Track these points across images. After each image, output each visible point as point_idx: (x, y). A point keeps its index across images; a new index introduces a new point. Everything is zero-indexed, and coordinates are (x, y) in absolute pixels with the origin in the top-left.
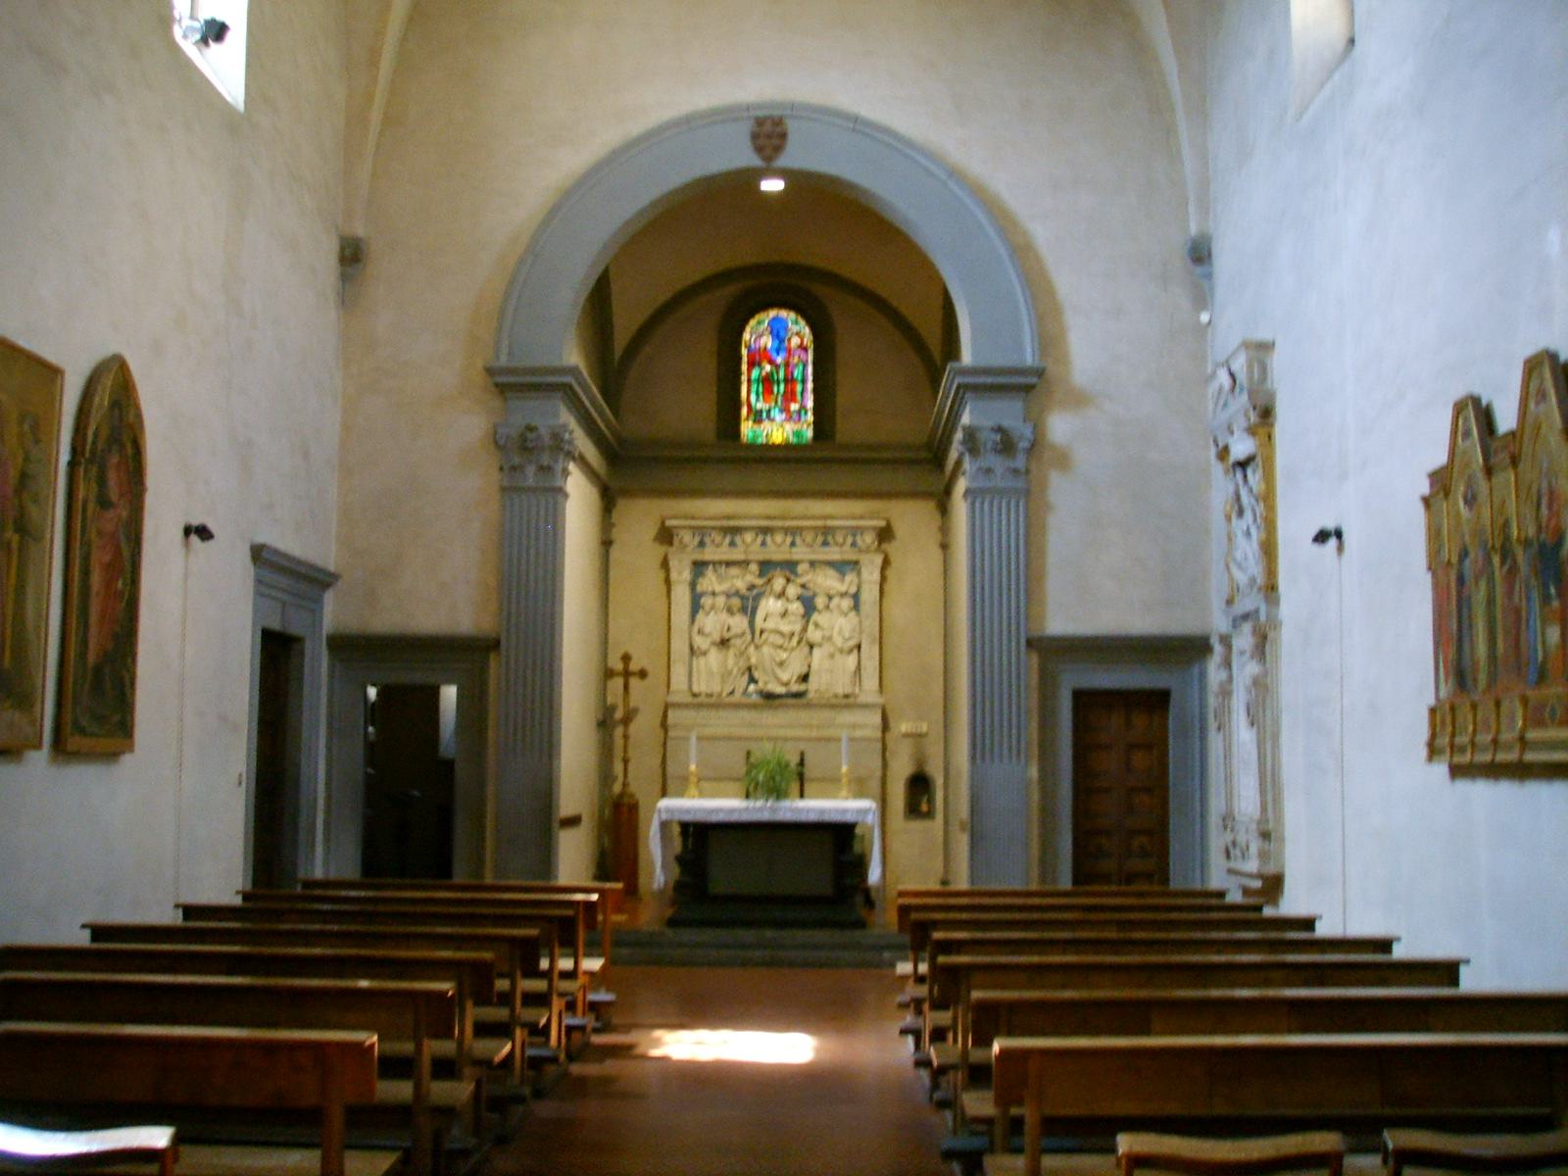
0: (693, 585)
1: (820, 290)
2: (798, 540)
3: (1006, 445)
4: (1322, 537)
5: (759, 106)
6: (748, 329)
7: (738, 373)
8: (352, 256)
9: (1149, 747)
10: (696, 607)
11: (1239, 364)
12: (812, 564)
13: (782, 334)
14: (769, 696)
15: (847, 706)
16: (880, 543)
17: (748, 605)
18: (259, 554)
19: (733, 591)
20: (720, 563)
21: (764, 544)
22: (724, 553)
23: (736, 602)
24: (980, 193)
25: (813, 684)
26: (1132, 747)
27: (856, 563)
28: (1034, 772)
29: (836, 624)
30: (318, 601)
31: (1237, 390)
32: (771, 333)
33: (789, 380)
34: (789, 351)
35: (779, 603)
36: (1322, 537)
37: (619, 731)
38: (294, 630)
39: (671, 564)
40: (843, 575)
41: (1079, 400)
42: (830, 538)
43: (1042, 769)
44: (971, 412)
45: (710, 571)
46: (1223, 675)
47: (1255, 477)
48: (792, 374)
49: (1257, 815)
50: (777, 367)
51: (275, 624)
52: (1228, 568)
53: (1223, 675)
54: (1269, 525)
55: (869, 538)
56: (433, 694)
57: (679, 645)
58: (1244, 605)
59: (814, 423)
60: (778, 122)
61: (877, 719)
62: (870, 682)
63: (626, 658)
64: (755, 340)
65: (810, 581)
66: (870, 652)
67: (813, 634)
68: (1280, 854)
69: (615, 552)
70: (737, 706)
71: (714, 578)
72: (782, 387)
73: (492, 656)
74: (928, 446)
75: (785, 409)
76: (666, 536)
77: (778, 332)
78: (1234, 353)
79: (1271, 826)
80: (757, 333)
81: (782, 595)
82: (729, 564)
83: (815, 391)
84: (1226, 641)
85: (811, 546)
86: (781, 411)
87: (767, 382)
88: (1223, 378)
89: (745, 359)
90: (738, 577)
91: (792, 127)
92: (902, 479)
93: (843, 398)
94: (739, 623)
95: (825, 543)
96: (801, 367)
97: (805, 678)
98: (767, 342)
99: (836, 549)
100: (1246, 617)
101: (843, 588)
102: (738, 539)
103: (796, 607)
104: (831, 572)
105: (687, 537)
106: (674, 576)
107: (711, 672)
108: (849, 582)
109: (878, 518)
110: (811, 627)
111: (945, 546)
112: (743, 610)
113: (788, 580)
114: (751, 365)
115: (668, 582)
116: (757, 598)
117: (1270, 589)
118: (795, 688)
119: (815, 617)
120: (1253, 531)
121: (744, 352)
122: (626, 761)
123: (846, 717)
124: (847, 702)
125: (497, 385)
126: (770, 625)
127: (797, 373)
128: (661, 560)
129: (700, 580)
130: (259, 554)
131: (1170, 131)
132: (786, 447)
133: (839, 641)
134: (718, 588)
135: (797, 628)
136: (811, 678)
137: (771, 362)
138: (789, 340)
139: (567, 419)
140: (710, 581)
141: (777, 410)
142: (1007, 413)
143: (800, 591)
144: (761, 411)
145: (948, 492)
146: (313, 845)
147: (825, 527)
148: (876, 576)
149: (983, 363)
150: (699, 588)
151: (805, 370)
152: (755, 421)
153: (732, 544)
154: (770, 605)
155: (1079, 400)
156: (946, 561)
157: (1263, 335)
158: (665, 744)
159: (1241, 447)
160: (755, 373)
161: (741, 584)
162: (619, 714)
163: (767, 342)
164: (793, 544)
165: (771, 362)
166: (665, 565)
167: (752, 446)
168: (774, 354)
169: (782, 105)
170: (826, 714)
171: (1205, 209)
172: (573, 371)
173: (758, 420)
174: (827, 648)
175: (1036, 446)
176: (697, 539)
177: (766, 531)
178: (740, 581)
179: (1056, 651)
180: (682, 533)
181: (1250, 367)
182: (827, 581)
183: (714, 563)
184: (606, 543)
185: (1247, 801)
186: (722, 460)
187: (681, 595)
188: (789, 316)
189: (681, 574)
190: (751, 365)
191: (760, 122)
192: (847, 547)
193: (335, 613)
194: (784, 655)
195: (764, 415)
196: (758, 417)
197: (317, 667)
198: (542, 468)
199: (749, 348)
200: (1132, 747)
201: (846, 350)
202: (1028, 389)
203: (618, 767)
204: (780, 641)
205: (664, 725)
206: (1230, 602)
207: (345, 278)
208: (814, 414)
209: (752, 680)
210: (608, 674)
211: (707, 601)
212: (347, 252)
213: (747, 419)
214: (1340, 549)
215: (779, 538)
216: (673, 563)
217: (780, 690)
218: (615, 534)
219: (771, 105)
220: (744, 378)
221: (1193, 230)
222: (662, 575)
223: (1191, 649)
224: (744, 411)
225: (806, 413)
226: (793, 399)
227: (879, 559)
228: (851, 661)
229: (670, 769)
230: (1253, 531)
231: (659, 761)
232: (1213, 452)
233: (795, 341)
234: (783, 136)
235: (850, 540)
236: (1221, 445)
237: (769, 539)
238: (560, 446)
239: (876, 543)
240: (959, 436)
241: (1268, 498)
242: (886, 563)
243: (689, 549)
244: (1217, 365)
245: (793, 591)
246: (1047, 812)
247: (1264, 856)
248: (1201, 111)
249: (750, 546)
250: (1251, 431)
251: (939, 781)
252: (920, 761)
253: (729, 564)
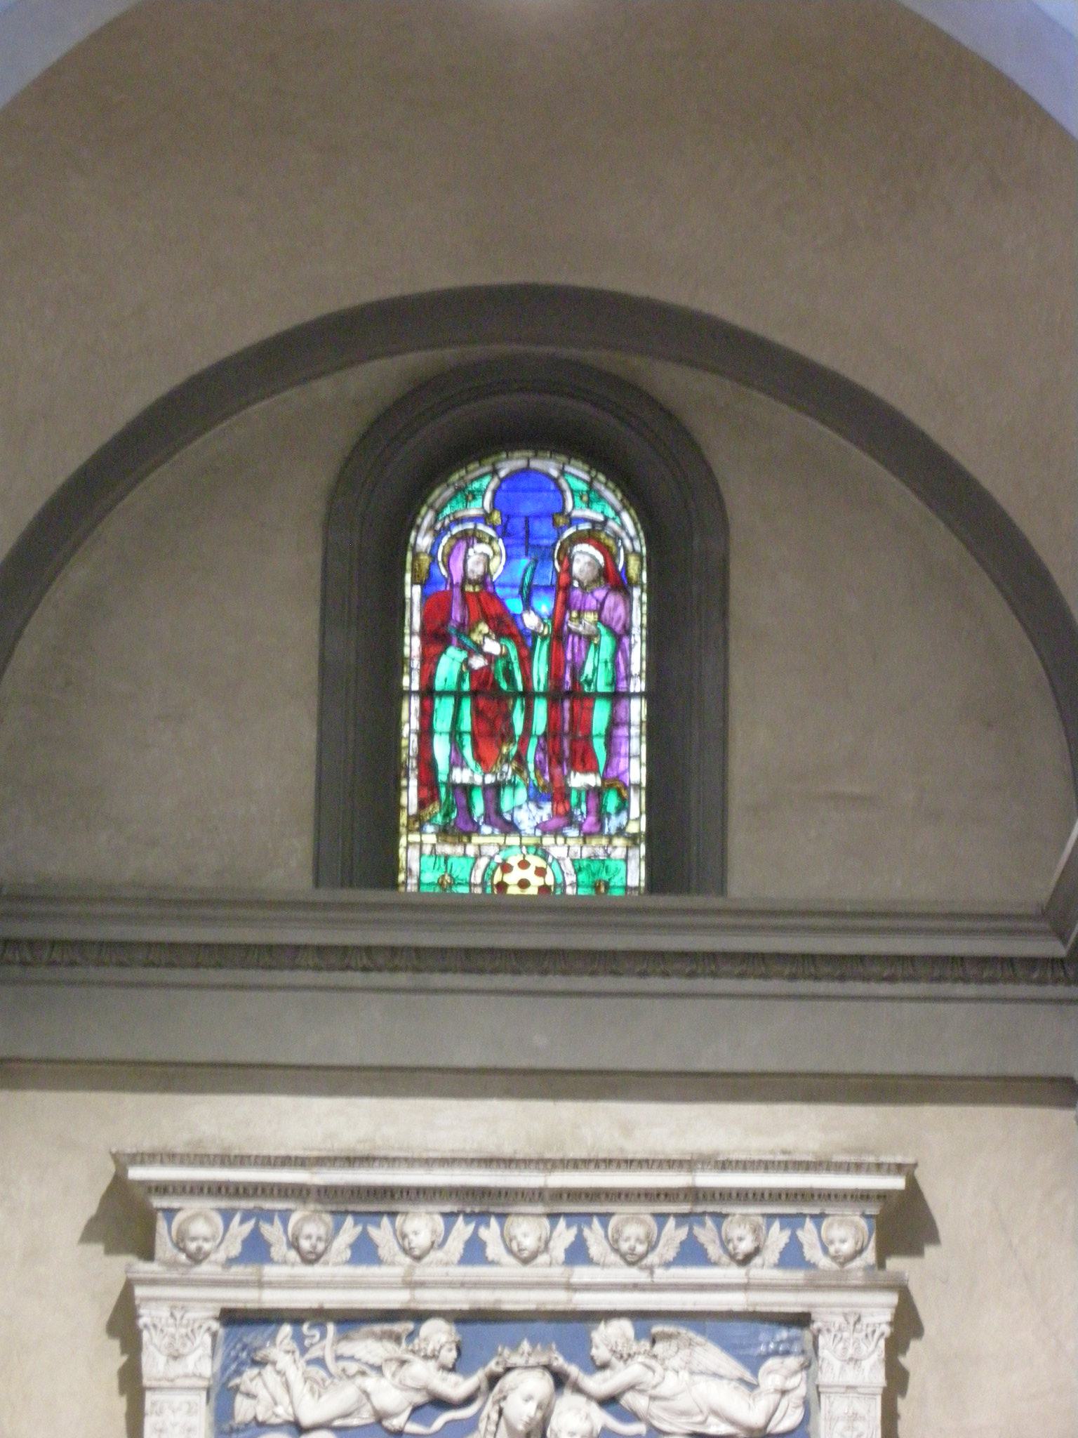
2: (595, 1237)
6: (427, 518)
7: (397, 663)
12: (640, 1317)
13: (542, 528)
16: (885, 1251)
19: (365, 1417)
20: (320, 1316)
21: (474, 1252)
27: (802, 1320)
32: (504, 532)
34: (563, 590)
39: (146, 1316)
40: (754, 1364)
42: (706, 1234)
48: (577, 670)
50: (525, 641)
59: (650, 836)
64: (448, 555)
65: (631, 1387)
71: (295, 1375)
72: (541, 708)
75: (559, 794)
83: (655, 730)
85: (633, 1260)
86: (536, 797)
89: (415, 618)
90: (379, 1369)
95: (692, 1253)
96: (607, 642)
99: (735, 1274)
102: (382, 1234)
104: (712, 1356)
106: (154, 1364)
109: (879, 1168)
113: (560, 1380)
114: (436, 639)
121: (413, 593)
128: (111, 1301)
129: (249, 1378)
134: (307, 1419)
137: (505, 626)
138: (567, 559)
141: (522, 793)
143: (601, 1418)
144: (467, 789)
147: (695, 1194)
148: (873, 1374)
150: (243, 1409)
152: (444, 832)
153: (364, 1251)
160: (449, 666)
164: (578, 1253)
165: (505, 626)
168: (515, 605)
176: (240, 1230)
180: (191, 1206)
183: (296, 1317)
188: (576, 477)
190: (436, 639)
192: (762, 1270)
195: (479, 808)
199: (426, 582)
208: (651, 810)
213: (418, 822)
215: (527, 1230)
220: (412, 682)
224: (410, 797)
225: (624, 806)
226: (584, 761)
233: (585, 558)
235: (778, 1237)
237: (491, 1233)
239: (870, 1256)
243: (206, 1270)
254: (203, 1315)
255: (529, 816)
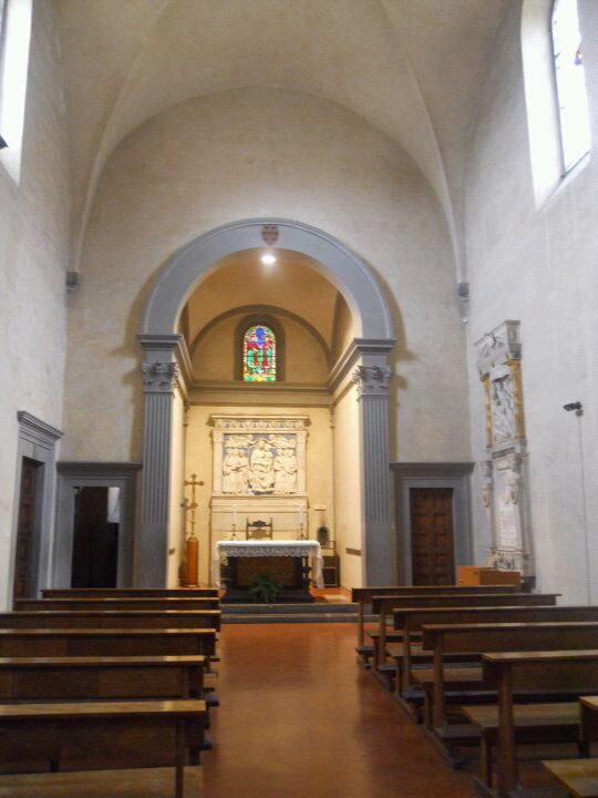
0: (224, 444)
1: (277, 316)
3: (379, 376)
4: (570, 407)
5: (265, 220)
8: (72, 281)
9: (443, 515)
10: (225, 454)
11: (502, 333)
14: (258, 493)
15: (291, 498)
17: (248, 452)
18: (21, 416)
22: (237, 430)
23: (242, 451)
24: (365, 262)
25: (277, 488)
26: (436, 515)
28: (393, 527)
29: (286, 461)
30: (53, 445)
31: (497, 346)
33: (265, 356)
34: (265, 344)
35: (262, 452)
36: (570, 407)
37: (189, 512)
38: (39, 459)
41: (409, 357)
43: (397, 524)
44: (363, 361)
45: (231, 438)
46: (488, 481)
47: (510, 387)
49: (520, 548)
51: (30, 456)
52: (489, 431)
53: (488, 481)
54: (520, 406)
55: (301, 424)
56: (104, 492)
57: (218, 471)
58: (498, 447)
60: (274, 227)
61: (303, 503)
62: (301, 487)
63: (194, 476)
66: (301, 473)
67: (277, 466)
68: (533, 567)
69: (189, 429)
70: (242, 498)
73: (139, 473)
74: (326, 385)
76: (211, 422)
77: (260, 334)
78: (497, 329)
79: (528, 552)
80: (251, 336)
81: (262, 449)
82: (240, 434)
84: (490, 464)
87: (255, 356)
88: (490, 341)
91: (280, 229)
92: (314, 399)
93: (289, 361)
94: (244, 461)
95: (282, 426)
97: (273, 485)
98: (255, 339)
100: (503, 453)
101: (289, 445)
103: (270, 454)
105: (220, 422)
106: (215, 440)
107: (232, 483)
108: (292, 443)
110: (276, 463)
111: (332, 428)
112: (246, 455)
114: (249, 349)
115: (212, 443)
116: (251, 450)
117: (522, 439)
118: (269, 489)
119: (278, 458)
120: (509, 411)
122: (193, 523)
123: (290, 502)
124: (291, 496)
125: (143, 344)
126: (258, 461)
127: (268, 353)
130: (21, 416)
131: (448, 237)
132: (263, 383)
133: (287, 469)
135: (269, 463)
136: (276, 485)
139: (174, 360)
140: (231, 442)
142: (379, 361)
145: (335, 404)
146: (46, 569)
148: (304, 441)
149: (366, 338)
151: (272, 352)
153: (242, 426)
154: (257, 453)
155: (409, 357)
156: (333, 436)
157: (513, 318)
158: (210, 515)
159: (499, 372)
161: (245, 444)
162: (189, 504)
163: (255, 339)
166: (211, 435)
167: (252, 383)
169: (277, 220)
170: (283, 501)
171: (465, 270)
172: (176, 337)
173: (251, 374)
174: (283, 472)
175: (393, 375)
177: (256, 420)
178: (245, 442)
179: (401, 471)
181: (509, 334)
182: (281, 442)
184: (185, 425)
185: (509, 537)
186: (236, 389)
187: (218, 448)
188: (265, 329)
189: (218, 438)
191: (266, 227)
193: (59, 452)
194: (264, 475)
196: (251, 371)
197: (51, 478)
198: (164, 383)
200: (436, 515)
201: (290, 344)
202: (388, 350)
203: (189, 525)
204: (263, 469)
205: (210, 507)
206: (489, 446)
207: (69, 292)
209: (250, 487)
210: (186, 483)
211: (229, 451)
212: (71, 280)
214: (580, 414)
215: (262, 423)
216: (215, 434)
217: (261, 490)
218: (189, 422)
219: (270, 219)
221: (459, 281)
222: (210, 439)
223: (465, 469)
224: (246, 368)
227: (304, 433)
228: (293, 478)
229: (214, 527)
230: (509, 411)
231: (207, 522)
232: (474, 376)
234: (276, 234)
236: (484, 373)
238: (170, 373)
240: (355, 369)
241: (519, 395)
242: (308, 435)
244: (486, 335)
245: (268, 447)
246: (400, 544)
247: (525, 567)
248: (462, 229)
249: (249, 427)
250: (509, 363)
251: (331, 531)
252: (323, 522)
253: (240, 434)
254: (221, 434)
255: (260, 371)
